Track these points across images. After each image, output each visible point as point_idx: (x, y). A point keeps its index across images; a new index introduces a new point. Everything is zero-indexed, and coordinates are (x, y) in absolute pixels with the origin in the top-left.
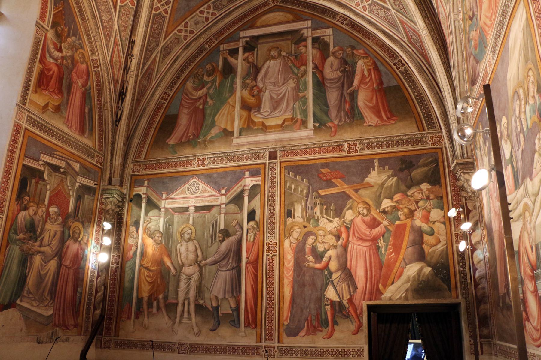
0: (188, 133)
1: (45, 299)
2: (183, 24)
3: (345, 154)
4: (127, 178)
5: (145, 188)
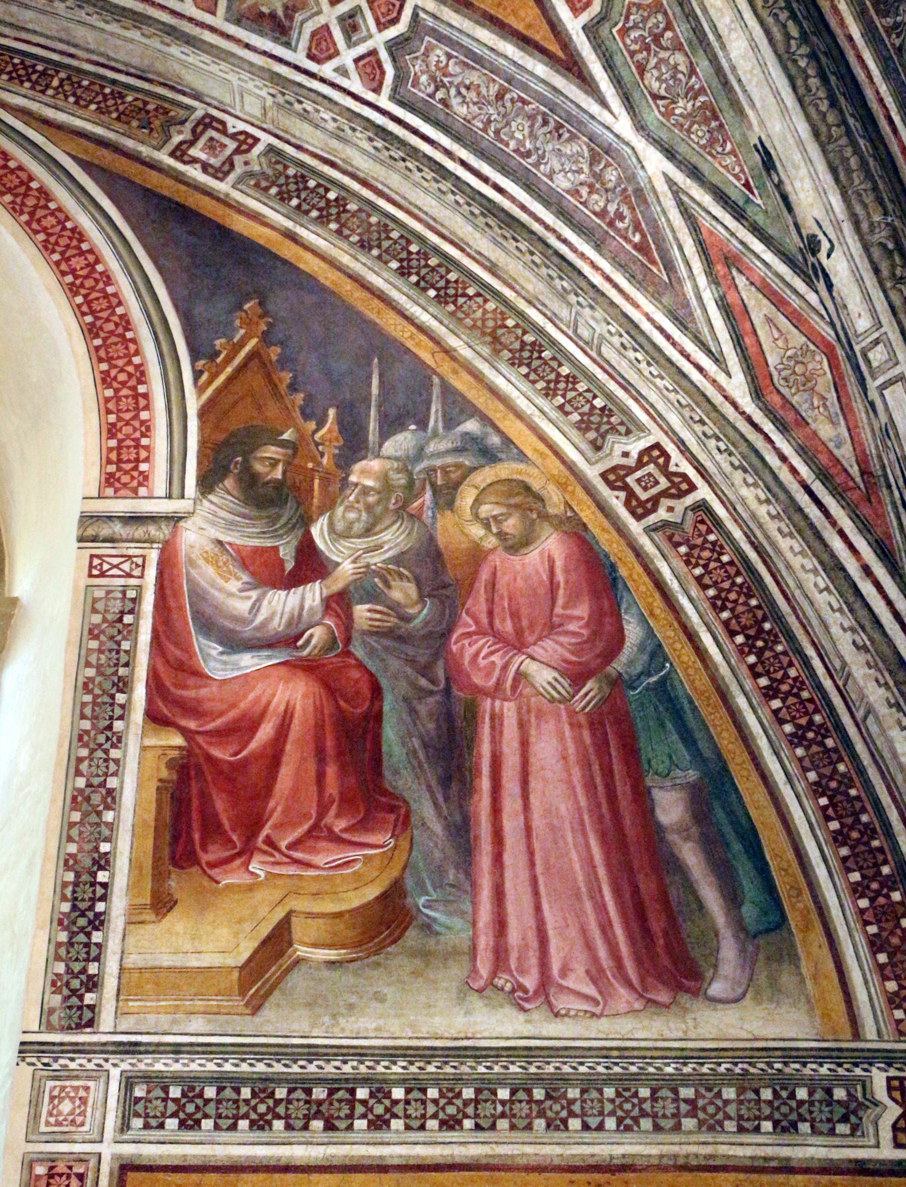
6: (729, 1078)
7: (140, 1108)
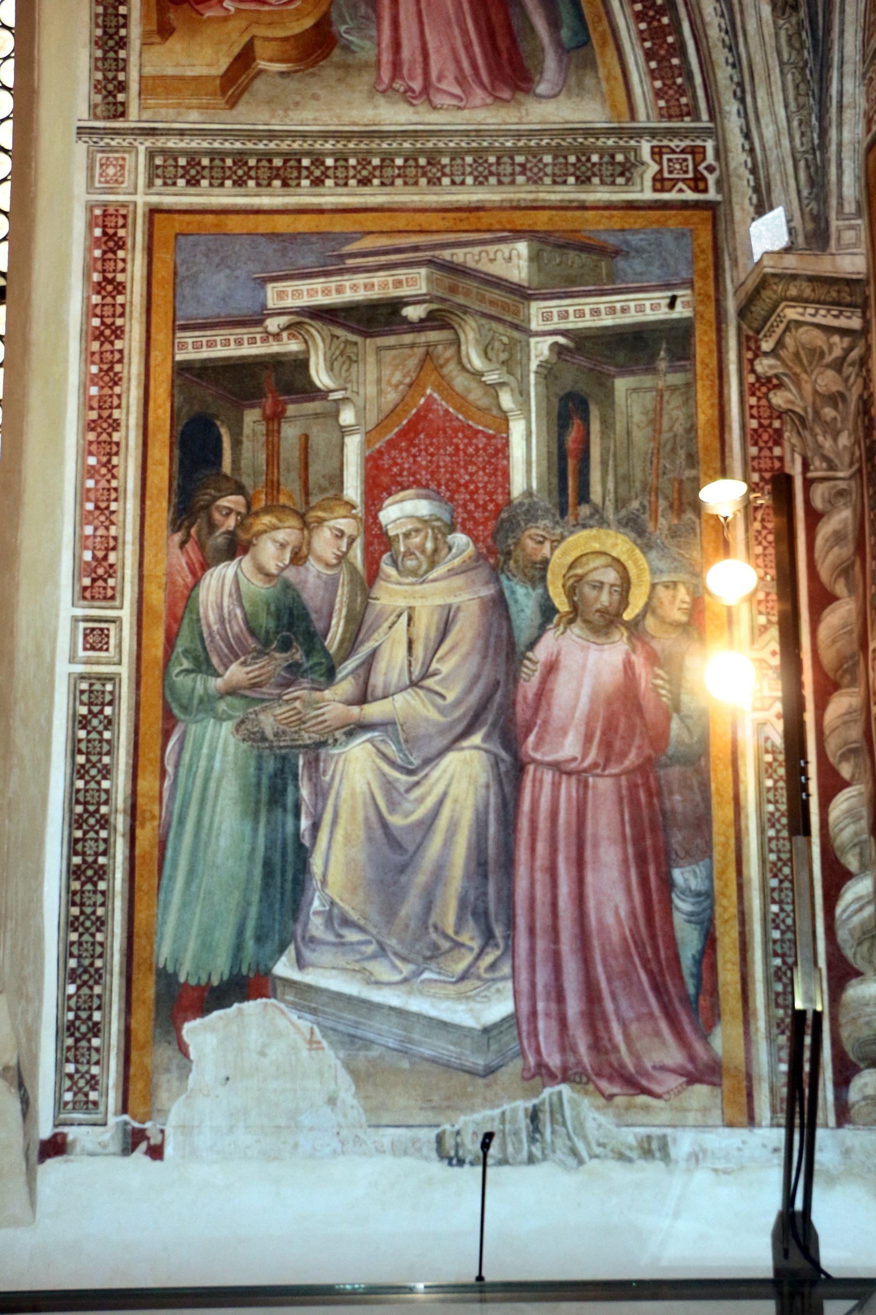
1: (445, 945)
6: (548, 149)
7: (160, 171)
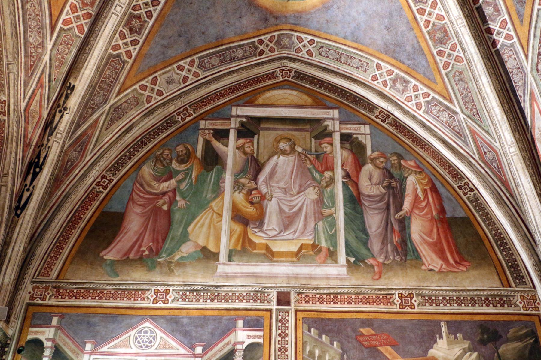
0: (140, 246)
2: (150, 78)
3: (395, 308)
4: (19, 309)
5: (53, 330)
